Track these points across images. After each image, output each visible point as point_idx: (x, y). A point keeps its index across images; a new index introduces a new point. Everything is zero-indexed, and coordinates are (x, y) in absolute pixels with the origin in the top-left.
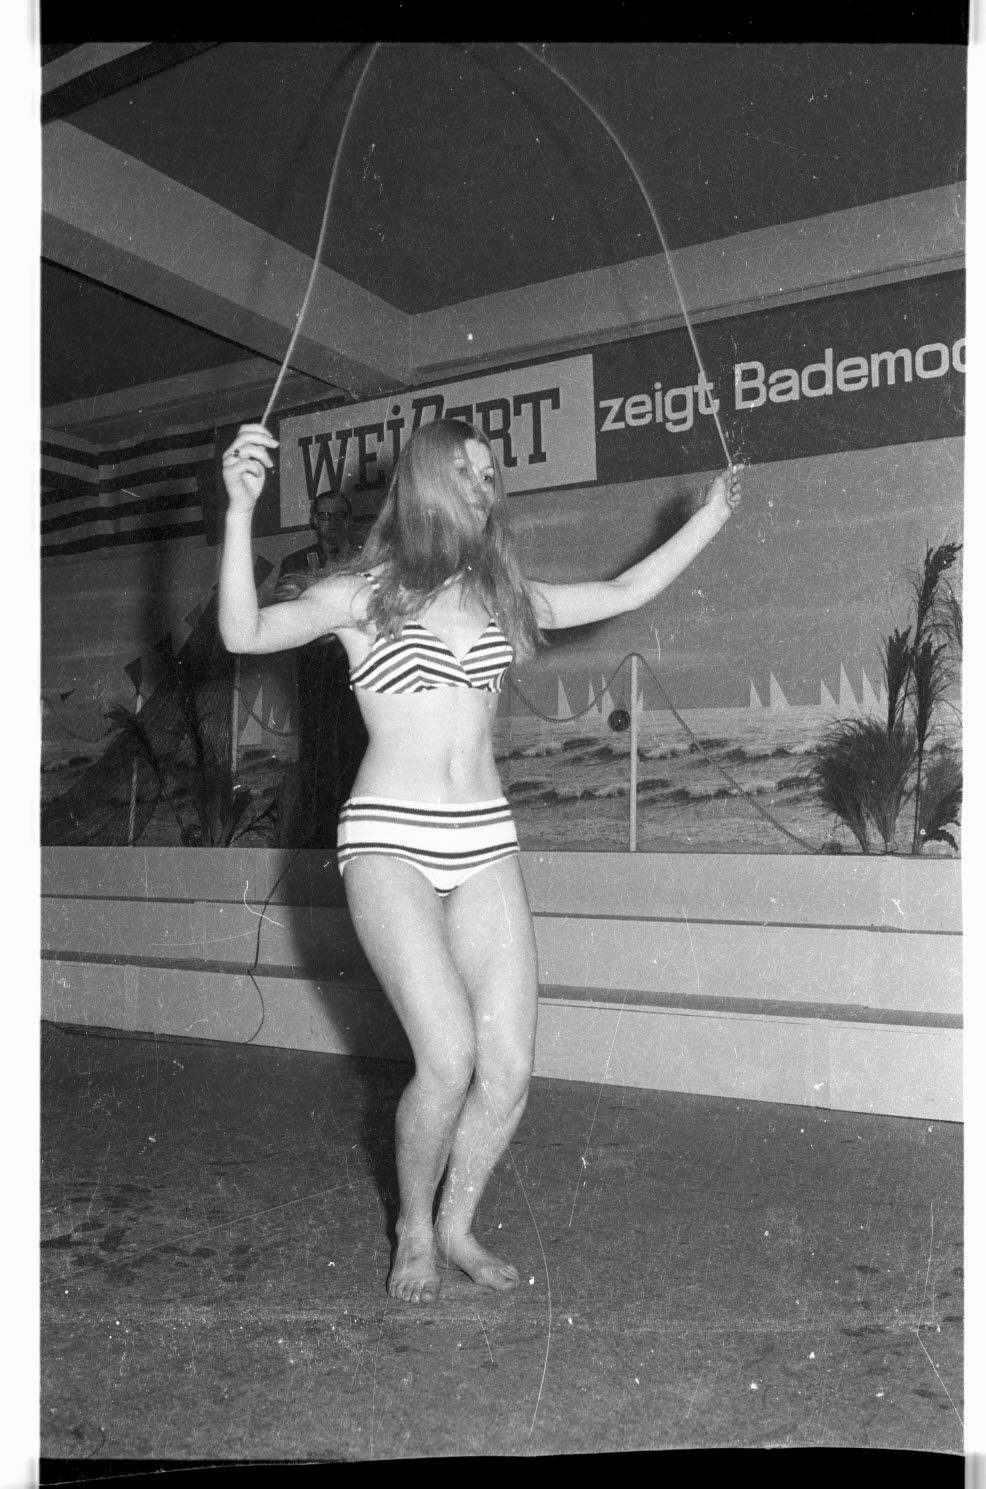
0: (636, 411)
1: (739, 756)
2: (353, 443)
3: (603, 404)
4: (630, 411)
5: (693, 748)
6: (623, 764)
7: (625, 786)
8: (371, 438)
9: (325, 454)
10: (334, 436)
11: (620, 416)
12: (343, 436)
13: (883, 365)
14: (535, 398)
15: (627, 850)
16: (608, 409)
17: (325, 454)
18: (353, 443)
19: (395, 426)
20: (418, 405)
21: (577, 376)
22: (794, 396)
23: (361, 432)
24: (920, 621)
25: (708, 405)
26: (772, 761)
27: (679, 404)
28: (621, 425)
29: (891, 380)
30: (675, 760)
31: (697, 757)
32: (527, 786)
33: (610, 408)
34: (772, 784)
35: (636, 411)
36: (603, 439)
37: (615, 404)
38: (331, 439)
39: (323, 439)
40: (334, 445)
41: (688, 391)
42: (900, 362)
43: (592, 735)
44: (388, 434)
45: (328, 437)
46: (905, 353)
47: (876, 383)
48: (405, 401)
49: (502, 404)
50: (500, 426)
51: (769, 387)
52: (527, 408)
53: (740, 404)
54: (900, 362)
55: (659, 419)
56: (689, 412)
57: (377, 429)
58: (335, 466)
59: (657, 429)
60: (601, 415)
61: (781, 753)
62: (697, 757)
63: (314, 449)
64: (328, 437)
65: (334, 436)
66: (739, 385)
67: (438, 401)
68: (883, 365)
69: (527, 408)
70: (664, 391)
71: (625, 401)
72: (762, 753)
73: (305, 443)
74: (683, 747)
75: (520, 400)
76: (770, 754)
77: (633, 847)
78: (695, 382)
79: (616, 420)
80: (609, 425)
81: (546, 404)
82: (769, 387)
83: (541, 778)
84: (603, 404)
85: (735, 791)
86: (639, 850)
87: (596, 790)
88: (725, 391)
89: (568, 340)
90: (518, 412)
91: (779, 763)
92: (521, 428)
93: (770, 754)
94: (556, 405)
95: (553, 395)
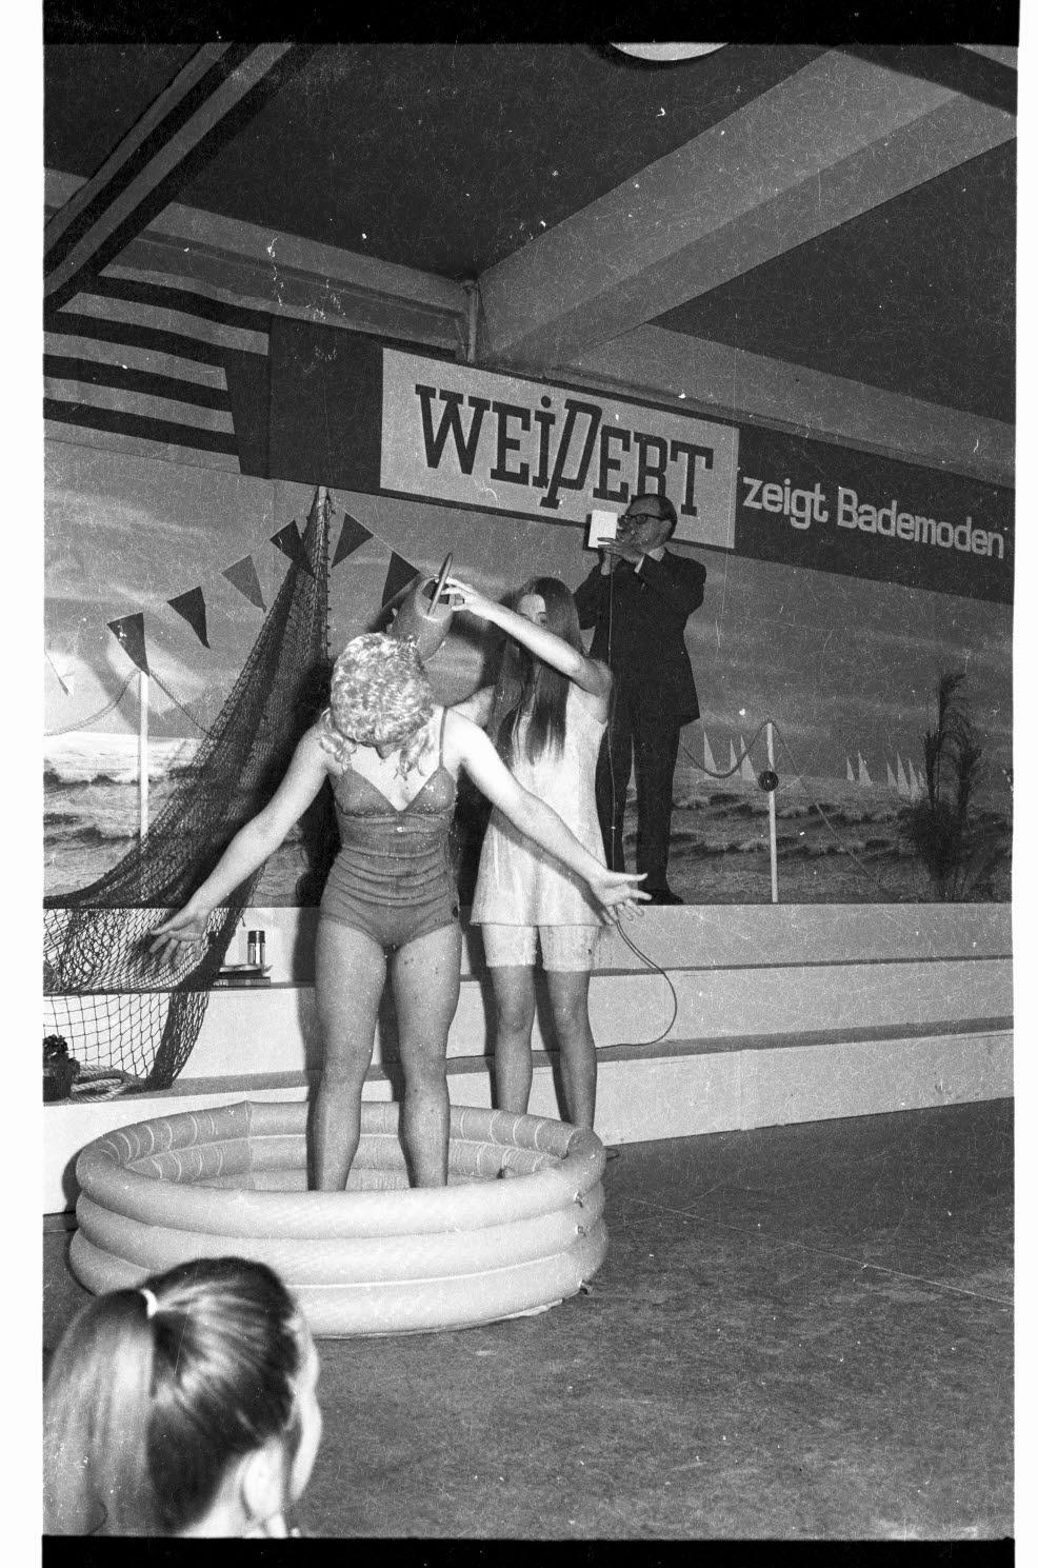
0: (779, 498)
1: (841, 821)
2: (491, 418)
3: (747, 480)
4: (766, 496)
5: (813, 810)
6: (762, 821)
7: (766, 841)
8: (514, 423)
9: (452, 416)
10: (466, 400)
11: (758, 498)
12: (480, 405)
13: (921, 526)
14: (694, 451)
15: (769, 902)
16: (750, 487)
17: (452, 416)
18: (491, 418)
19: (547, 420)
20: (574, 407)
21: (726, 442)
22: (872, 529)
23: (504, 410)
24: (941, 729)
25: (821, 514)
26: (91, 788)
27: (801, 503)
28: (757, 506)
29: (925, 541)
30: (798, 820)
31: (814, 819)
32: (68, 819)
33: (750, 487)
34: (861, 844)
35: (779, 498)
36: (743, 514)
37: (756, 484)
38: (461, 402)
39: (453, 399)
40: (467, 412)
41: (807, 495)
42: (930, 526)
43: (735, 791)
44: (536, 426)
45: (459, 398)
46: (932, 521)
47: (917, 539)
48: (560, 397)
50: (657, 465)
51: (860, 515)
52: (684, 456)
53: (841, 522)
54: (930, 526)
55: (786, 512)
56: (807, 514)
57: (523, 413)
58: (466, 440)
59: (782, 519)
60: (743, 491)
61: (867, 819)
62: (814, 819)
63: (439, 407)
64: (459, 398)
65: (466, 400)
66: (842, 507)
67: (596, 412)
68: (921, 526)
69: (684, 456)
70: (793, 487)
71: (763, 485)
72: (80, 779)
73: (425, 393)
74: (803, 809)
75: (678, 446)
76: (90, 781)
77: (775, 899)
78: (813, 490)
79: (758, 498)
80: (749, 502)
81: (701, 461)
82: (860, 515)
83: (690, 831)
84: (747, 480)
85: (842, 849)
86: (780, 902)
87: (739, 845)
88: (830, 505)
89: (658, 392)
90: (674, 458)
91: (864, 827)
93: (90, 781)
94: (709, 465)
95: (708, 453)
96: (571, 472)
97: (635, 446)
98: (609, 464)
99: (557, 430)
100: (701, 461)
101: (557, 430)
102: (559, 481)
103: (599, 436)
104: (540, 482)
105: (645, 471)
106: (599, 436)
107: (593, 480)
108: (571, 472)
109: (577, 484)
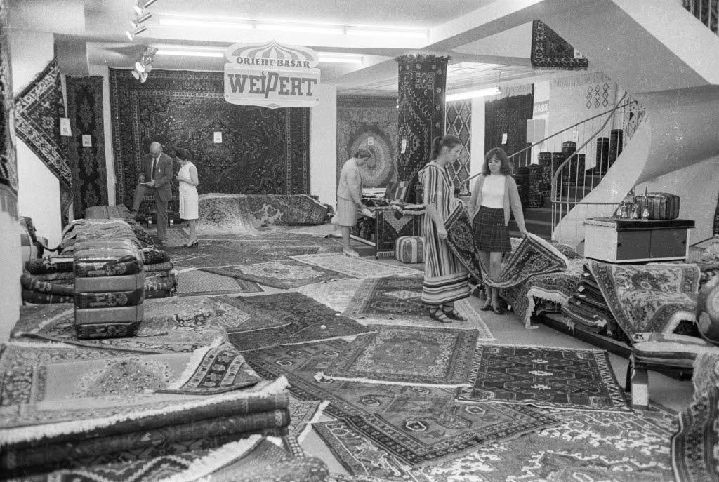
2: (248, 81)
9: (238, 81)
17: (238, 81)
18: (248, 81)
40: (241, 79)
49: (298, 79)
52: (306, 82)
63: (234, 79)
69: (306, 82)
75: (304, 80)
81: (312, 83)
92: (304, 87)
96: (271, 87)
97: (291, 81)
98: (283, 86)
99: (266, 81)
100: (312, 83)
101: (266, 81)
102: (269, 89)
103: (279, 81)
104: (263, 92)
105: (294, 87)
106: (279, 81)
107: (278, 89)
108: (271, 87)
109: (274, 90)
